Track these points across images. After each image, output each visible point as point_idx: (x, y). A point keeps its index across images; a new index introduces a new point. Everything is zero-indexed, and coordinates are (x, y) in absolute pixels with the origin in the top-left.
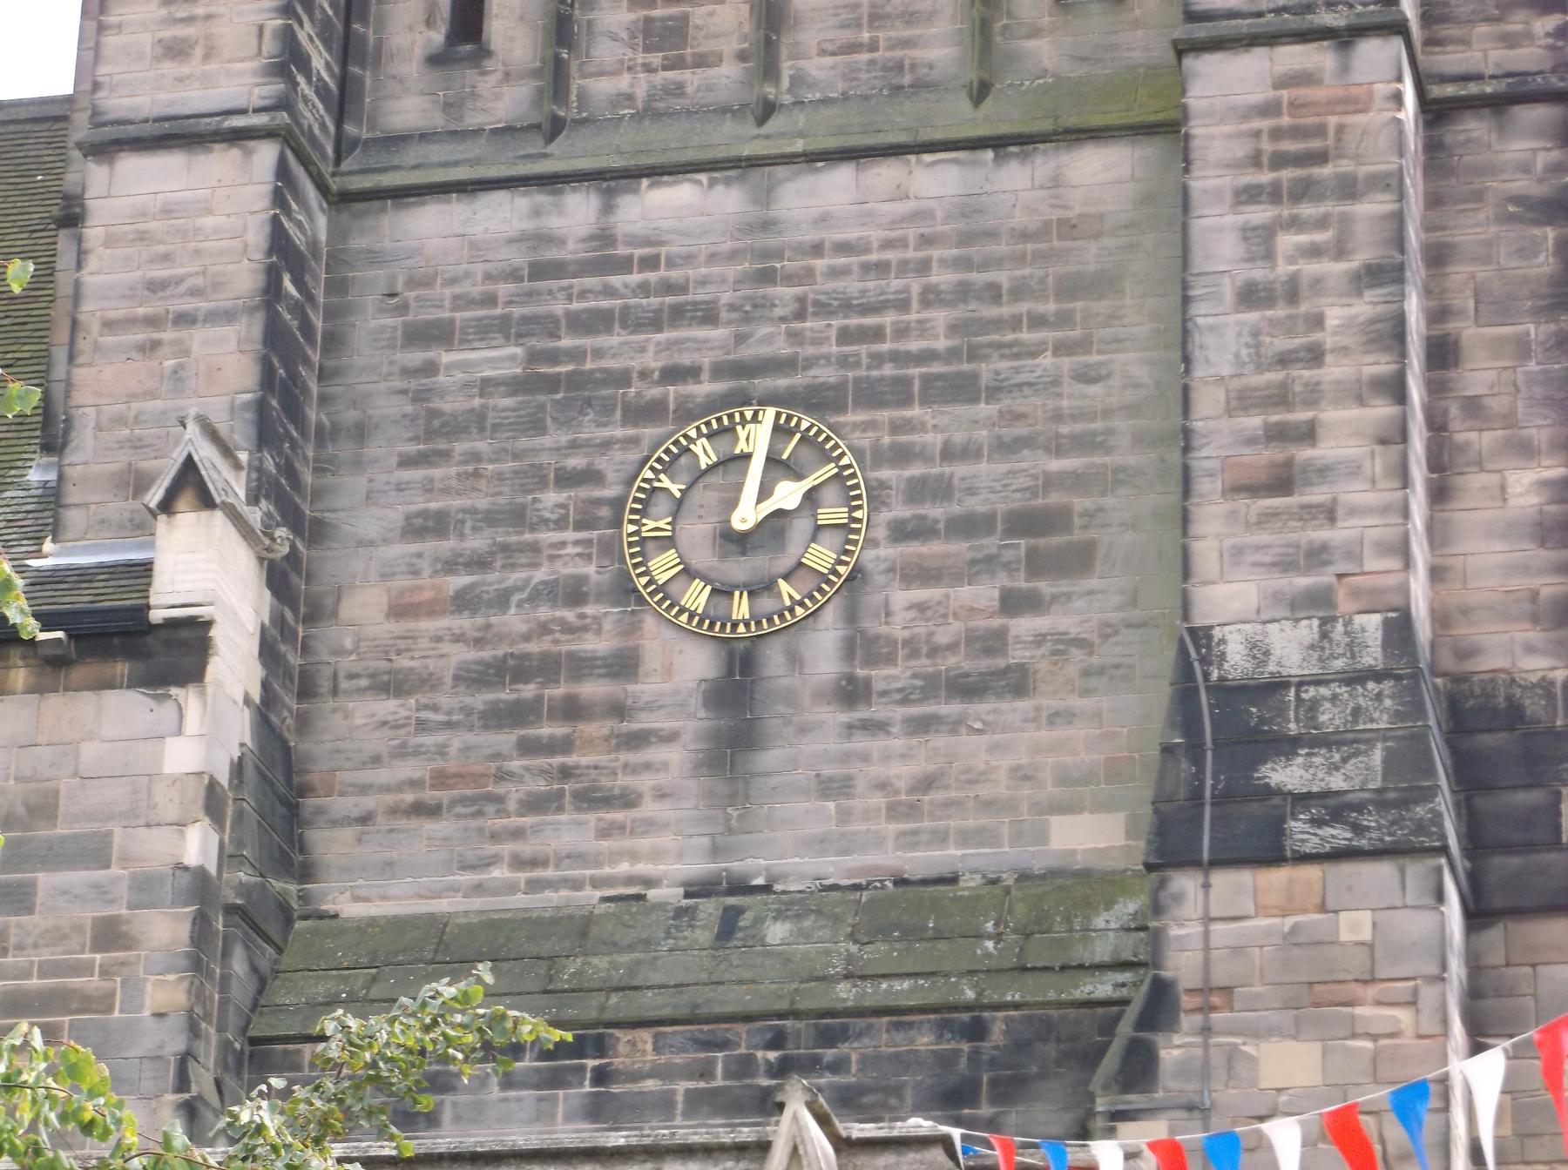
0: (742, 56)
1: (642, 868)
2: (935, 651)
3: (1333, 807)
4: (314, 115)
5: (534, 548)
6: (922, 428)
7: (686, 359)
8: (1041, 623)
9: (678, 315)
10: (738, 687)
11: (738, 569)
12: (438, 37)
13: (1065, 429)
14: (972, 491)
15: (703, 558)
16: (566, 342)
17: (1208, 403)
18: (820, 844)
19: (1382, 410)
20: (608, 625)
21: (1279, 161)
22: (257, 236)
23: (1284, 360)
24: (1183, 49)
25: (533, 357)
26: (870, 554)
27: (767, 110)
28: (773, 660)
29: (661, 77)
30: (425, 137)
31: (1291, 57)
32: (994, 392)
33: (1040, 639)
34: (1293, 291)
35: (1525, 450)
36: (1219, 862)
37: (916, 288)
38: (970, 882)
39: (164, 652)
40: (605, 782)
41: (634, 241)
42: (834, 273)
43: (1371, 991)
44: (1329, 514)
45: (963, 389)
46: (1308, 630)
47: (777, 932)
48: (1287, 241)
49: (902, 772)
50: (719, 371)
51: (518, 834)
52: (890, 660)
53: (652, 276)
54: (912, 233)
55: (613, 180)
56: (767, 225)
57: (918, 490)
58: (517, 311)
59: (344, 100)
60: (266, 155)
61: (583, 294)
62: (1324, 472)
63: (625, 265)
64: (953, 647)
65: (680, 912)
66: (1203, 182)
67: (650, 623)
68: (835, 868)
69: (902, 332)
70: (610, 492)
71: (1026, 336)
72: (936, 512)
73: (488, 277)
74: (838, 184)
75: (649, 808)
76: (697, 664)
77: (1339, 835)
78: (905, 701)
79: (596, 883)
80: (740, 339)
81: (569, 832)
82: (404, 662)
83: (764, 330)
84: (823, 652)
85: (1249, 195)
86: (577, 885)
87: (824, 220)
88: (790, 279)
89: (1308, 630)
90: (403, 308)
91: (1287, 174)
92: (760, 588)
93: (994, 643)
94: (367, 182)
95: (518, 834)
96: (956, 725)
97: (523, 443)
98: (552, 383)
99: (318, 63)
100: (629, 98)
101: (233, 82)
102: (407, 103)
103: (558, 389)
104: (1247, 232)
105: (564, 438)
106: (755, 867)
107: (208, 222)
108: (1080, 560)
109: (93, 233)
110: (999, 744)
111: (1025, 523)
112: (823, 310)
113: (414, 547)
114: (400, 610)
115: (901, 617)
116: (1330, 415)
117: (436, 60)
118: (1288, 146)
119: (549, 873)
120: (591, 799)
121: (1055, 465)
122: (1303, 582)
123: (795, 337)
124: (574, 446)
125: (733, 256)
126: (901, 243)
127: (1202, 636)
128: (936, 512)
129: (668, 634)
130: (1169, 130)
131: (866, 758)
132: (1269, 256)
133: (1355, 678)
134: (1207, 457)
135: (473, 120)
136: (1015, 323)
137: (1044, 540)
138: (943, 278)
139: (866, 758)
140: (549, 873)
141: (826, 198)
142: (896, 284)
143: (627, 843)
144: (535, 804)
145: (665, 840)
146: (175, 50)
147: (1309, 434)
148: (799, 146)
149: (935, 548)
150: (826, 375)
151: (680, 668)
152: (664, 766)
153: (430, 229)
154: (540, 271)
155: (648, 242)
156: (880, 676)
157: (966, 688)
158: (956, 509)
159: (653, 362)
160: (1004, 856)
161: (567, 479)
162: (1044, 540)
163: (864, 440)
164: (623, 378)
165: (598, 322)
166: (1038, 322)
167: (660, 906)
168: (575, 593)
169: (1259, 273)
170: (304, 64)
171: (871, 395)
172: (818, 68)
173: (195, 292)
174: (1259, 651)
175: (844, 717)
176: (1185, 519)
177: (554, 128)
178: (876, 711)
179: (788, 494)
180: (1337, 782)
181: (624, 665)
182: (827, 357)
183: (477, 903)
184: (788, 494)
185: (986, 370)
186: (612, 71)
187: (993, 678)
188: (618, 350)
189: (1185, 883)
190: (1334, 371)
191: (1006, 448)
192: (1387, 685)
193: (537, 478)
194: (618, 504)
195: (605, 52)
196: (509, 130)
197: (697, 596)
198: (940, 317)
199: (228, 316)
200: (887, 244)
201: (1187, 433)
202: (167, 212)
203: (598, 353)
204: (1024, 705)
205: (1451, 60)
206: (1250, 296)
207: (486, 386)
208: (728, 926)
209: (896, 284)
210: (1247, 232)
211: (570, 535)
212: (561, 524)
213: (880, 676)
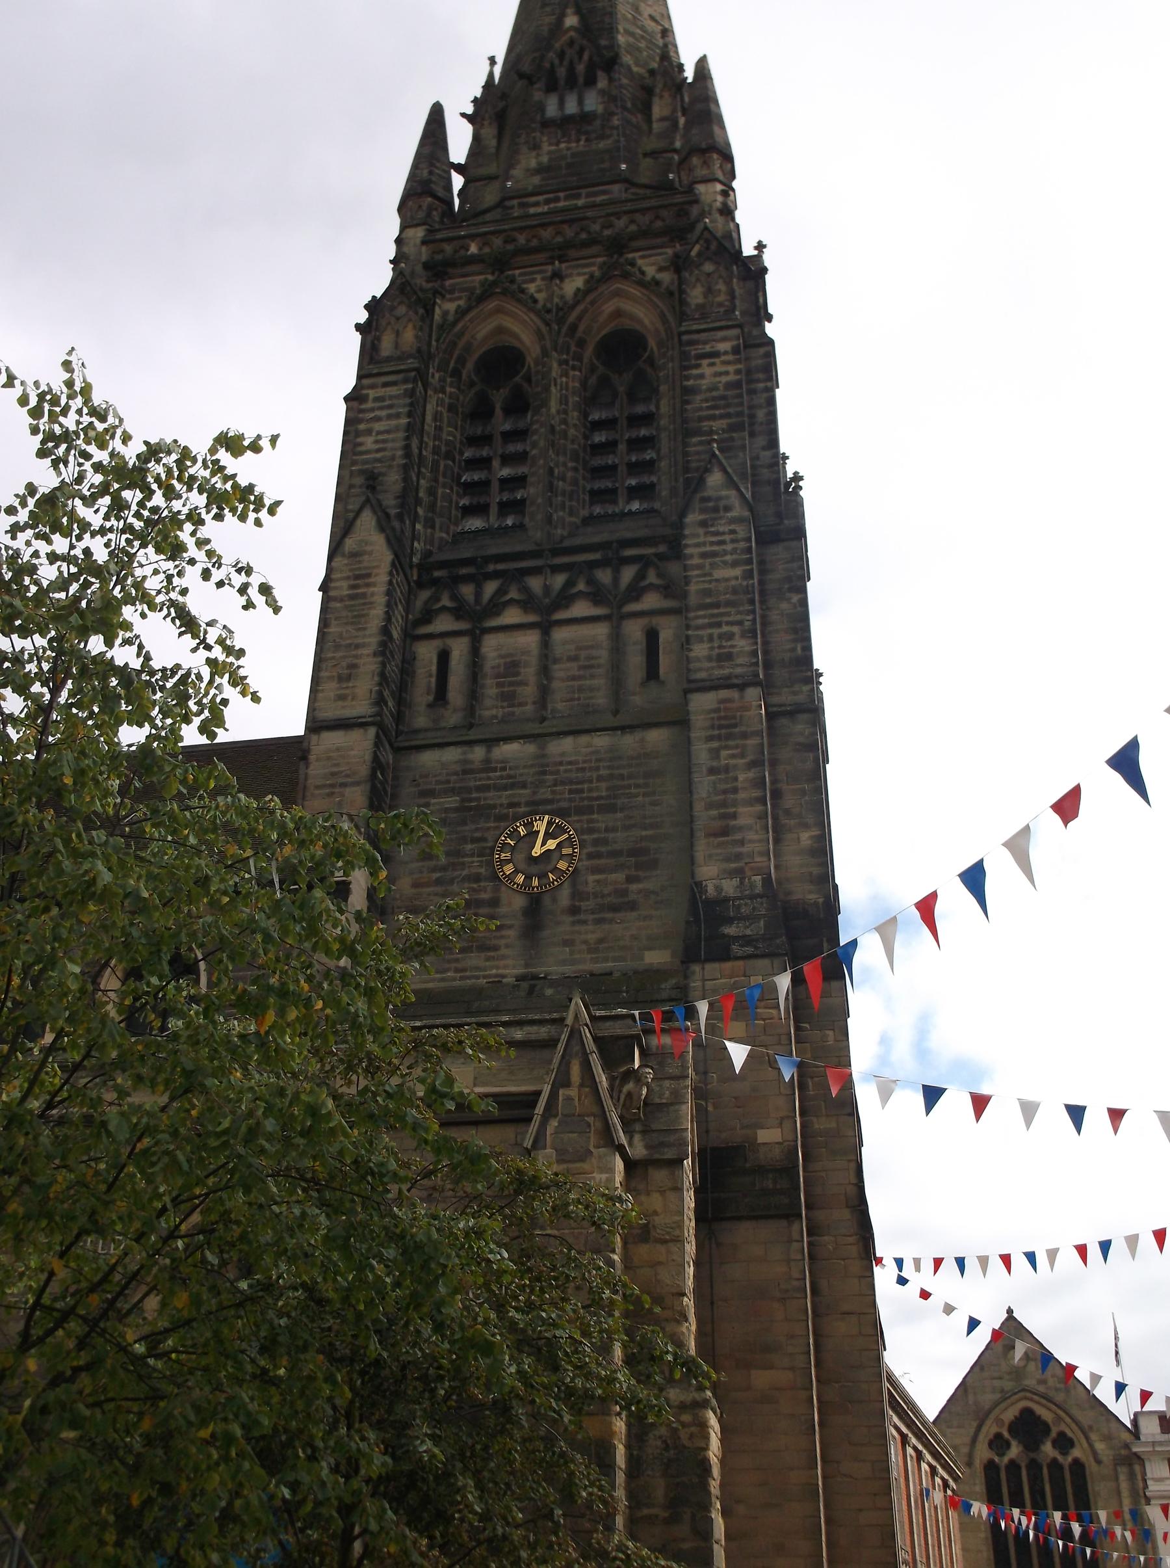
0: (534, 703)
1: (500, 971)
2: (603, 896)
3: (747, 941)
4: (389, 721)
5: (463, 864)
6: (598, 821)
7: (516, 800)
8: (641, 886)
9: (513, 786)
10: (535, 907)
11: (534, 869)
12: (431, 698)
13: (647, 821)
14: (615, 842)
15: (522, 866)
16: (474, 795)
17: (698, 807)
18: (564, 962)
19: (759, 808)
20: (489, 889)
21: (720, 727)
22: (368, 757)
23: (725, 792)
24: (686, 692)
25: (463, 800)
26: (580, 864)
27: (543, 719)
28: (547, 900)
29: (506, 710)
30: (426, 730)
31: (724, 694)
32: (622, 810)
33: (640, 891)
34: (727, 769)
35: (806, 826)
36: (707, 960)
37: (595, 775)
38: (616, 975)
40: (488, 942)
41: (497, 762)
42: (566, 771)
43: (763, 1004)
44: (742, 843)
45: (611, 809)
46: (736, 882)
47: (549, 992)
48: (724, 753)
49: (592, 937)
50: (527, 804)
51: (457, 960)
52: (588, 900)
53: (504, 773)
54: (594, 758)
55: (491, 742)
56: (544, 756)
57: (596, 842)
58: (457, 785)
59: (399, 718)
60: (372, 731)
61: (480, 780)
62: (740, 829)
63: (495, 770)
64: (609, 895)
65: (514, 986)
66: (694, 735)
67: (503, 888)
68: (568, 970)
69: (590, 790)
70: (489, 844)
71: (633, 791)
72: (603, 849)
73: (448, 774)
74: (567, 743)
75: (503, 951)
76: (519, 902)
77: (749, 950)
78: (593, 913)
79: (485, 977)
80: (534, 793)
81: (474, 959)
82: (417, 903)
83: (543, 790)
84: (564, 897)
85: (710, 738)
86: (478, 978)
87: (563, 754)
88: (551, 773)
89: (736, 882)
90: (419, 785)
91: (723, 731)
92: (542, 876)
93: (624, 893)
94: (407, 744)
95: (457, 960)
96: (611, 921)
97: (459, 829)
98: (470, 809)
99: (390, 704)
100: (496, 717)
101: (361, 707)
102: (421, 721)
104: (711, 750)
105: (473, 827)
106: (541, 970)
107: (353, 753)
108: (654, 864)
109: (312, 758)
111: (634, 852)
112: (563, 783)
113: (420, 864)
114: (416, 885)
115: (591, 885)
116: (741, 810)
117: (430, 706)
118: (723, 722)
119: (468, 974)
120: (483, 948)
121: (644, 833)
122: (733, 865)
123: (553, 792)
124: (477, 829)
125: (532, 766)
126: (590, 761)
127: (699, 884)
128: (603, 849)
129: (510, 892)
130: (682, 723)
131: (579, 933)
132: (718, 757)
133: (752, 897)
134: (699, 824)
135: (443, 724)
136: (629, 787)
137: (641, 859)
138: (603, 772)
139: (579, 933)
140: (468, 974)
142: (588, 774)
143: (496, 963)
144: (463, 950)
145: (509, 962)
146: (342, 698)
147: (734, 816)
148: (554, 730)
149: (603, 861)
150: (564, 804)
152: (509, 937)
153: (429, 758)
154: (465, 772)
155: (502, 762)
156: (584, 905)
157: (615, 909)
158: (609, 848)
159: (505, 802)
161: (474, 840)
162: (641, 859)
163: (578, 825)
164: (494, 807)
165: (486, 788)
166: (637, 786)
167: (508, 984)
168: (477, 878)
169: (715, 764)
170: (386, 704)
171: (580, 811)
172: (560, 706)
173: (348, 776)
174: (719, 889)
175: (571, 919)
176: (692, 845)
177: (471, 726)
178: (582, 917)
179: (552, 844)
180: (748, 932)
181: (495, 902)
182: (565, 799)
183: (442, 984)
184: (552, 844)
185: (619, 802)
186: (491, 708)
187: (623, 904)
188: (492, 798)
189: (696, 968)
190: (742, 795)
191: (627, 828)
192: (764, 900)
193: (464, 840)
194: (492, 849)
195: (488, 702)
196: (455, 727)
197: (520, 879)
198: (603, 785)
199: (357, 784)
200: (584, 762)
201: (692, 816)
202: (338, 749)
203: (485, 799)
204: (635, 914)
205: (775, 700)
206: (712, 771)
207: (446, 810)
208: (531, 990)
209: (588, 774)
210: (711, 750)
211: (476, 859)
212: (472, 855)
213: (584, 905)
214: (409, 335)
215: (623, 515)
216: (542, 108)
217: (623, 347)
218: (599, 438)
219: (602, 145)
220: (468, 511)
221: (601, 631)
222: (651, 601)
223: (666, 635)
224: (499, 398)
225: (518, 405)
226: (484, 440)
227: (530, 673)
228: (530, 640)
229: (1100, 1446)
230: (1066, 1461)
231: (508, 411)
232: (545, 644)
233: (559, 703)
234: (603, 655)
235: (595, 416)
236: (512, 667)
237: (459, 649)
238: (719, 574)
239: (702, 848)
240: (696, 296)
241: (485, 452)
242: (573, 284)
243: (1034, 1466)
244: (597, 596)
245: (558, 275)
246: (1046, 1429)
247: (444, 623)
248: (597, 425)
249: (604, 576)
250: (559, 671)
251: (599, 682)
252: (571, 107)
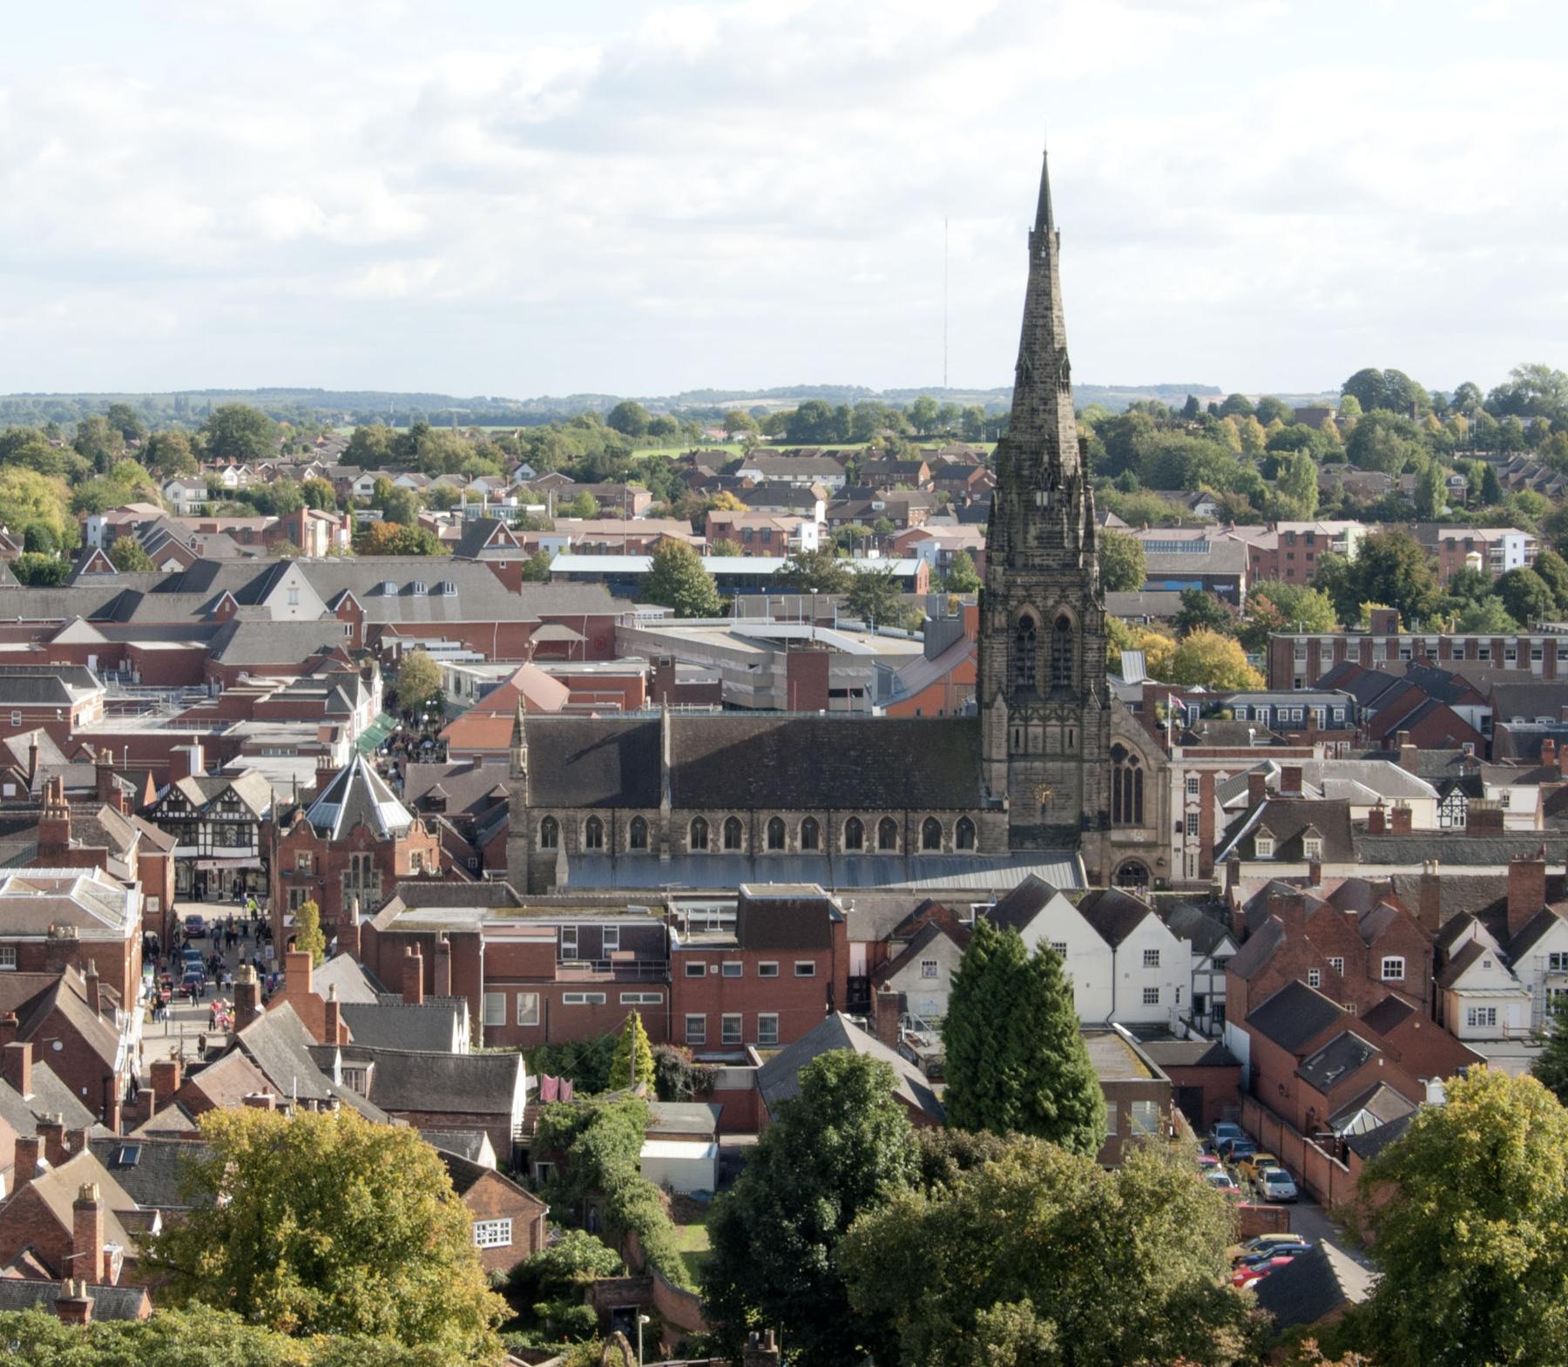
10: (1044, 807)
39: (1004, 812)
103: (1028, 780)
110: (1064, 813)
137: (1068, 796)
141: (1050, 765)
151: (1039, 806)
187: (1063, 808)
214: (1004, 619)
217: (1063, 622)
222: (1071, 722)
225: (1032, 637)
227: (1040, 740)
229: (1152, 762)
230: (1133, 769)
236: (1036, 738)
237: (1022, 730)
242: (1050, 602)
243: (1118, 771)
246: (1126, 753)
247: (1017, 722)
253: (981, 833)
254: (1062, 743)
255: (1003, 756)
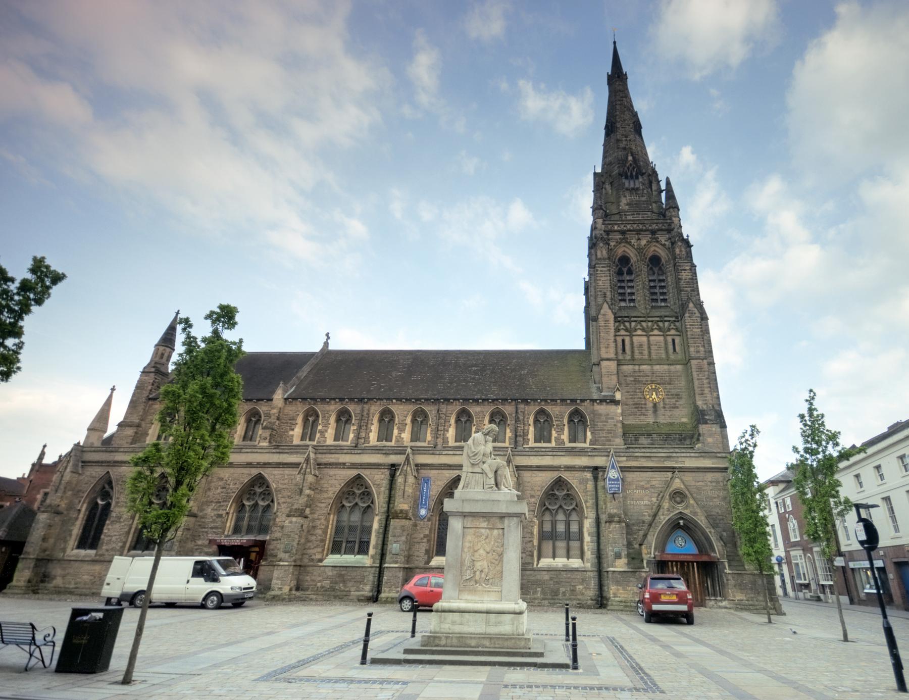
55: (639, 365)
74: (658, 367)
76: (651, 405)
81: (642, 417)
84: (662, 405)
108: (681, 398)
110: (676, 412)
137: (678, 396)
141: (657, 368)
153: (625, 368)
160: (678, 421)
186: (637, 356)
214: (605, 252)
215: (661, 307)
216: (624, 184)
217: (655, 261)
218: (652, 284)
219: (644, 199)
220: (620, 300)
221: (662, 338)
222: (673, 332)
223: (677, 341)
224: (625, 270)
225: (630, 272)
226: (623, 281)
227: (645, 347)
228: (645, 339)
231: (627, 274)
232: (649, 341)
233: (654, 356)
234: (663, 345)
235: (651, 278)
236: (641, 345)
237: (627, 339)
238: (695, 330)
239: (697, 397)
240: (677, 251)
241: (623, 284)
242: (643, 242)
244: (660, 329)
245: (639, 239)
248: (650, 281)
249: (661, 324)
250: (652, 347)
251: (663, 351)
252: (632, 186)
253: (594, 425)
254: (666, 349)
255: (612, 356)
